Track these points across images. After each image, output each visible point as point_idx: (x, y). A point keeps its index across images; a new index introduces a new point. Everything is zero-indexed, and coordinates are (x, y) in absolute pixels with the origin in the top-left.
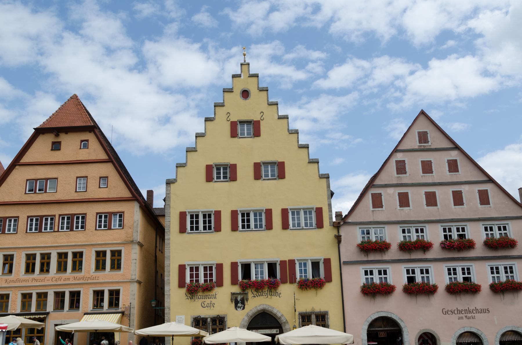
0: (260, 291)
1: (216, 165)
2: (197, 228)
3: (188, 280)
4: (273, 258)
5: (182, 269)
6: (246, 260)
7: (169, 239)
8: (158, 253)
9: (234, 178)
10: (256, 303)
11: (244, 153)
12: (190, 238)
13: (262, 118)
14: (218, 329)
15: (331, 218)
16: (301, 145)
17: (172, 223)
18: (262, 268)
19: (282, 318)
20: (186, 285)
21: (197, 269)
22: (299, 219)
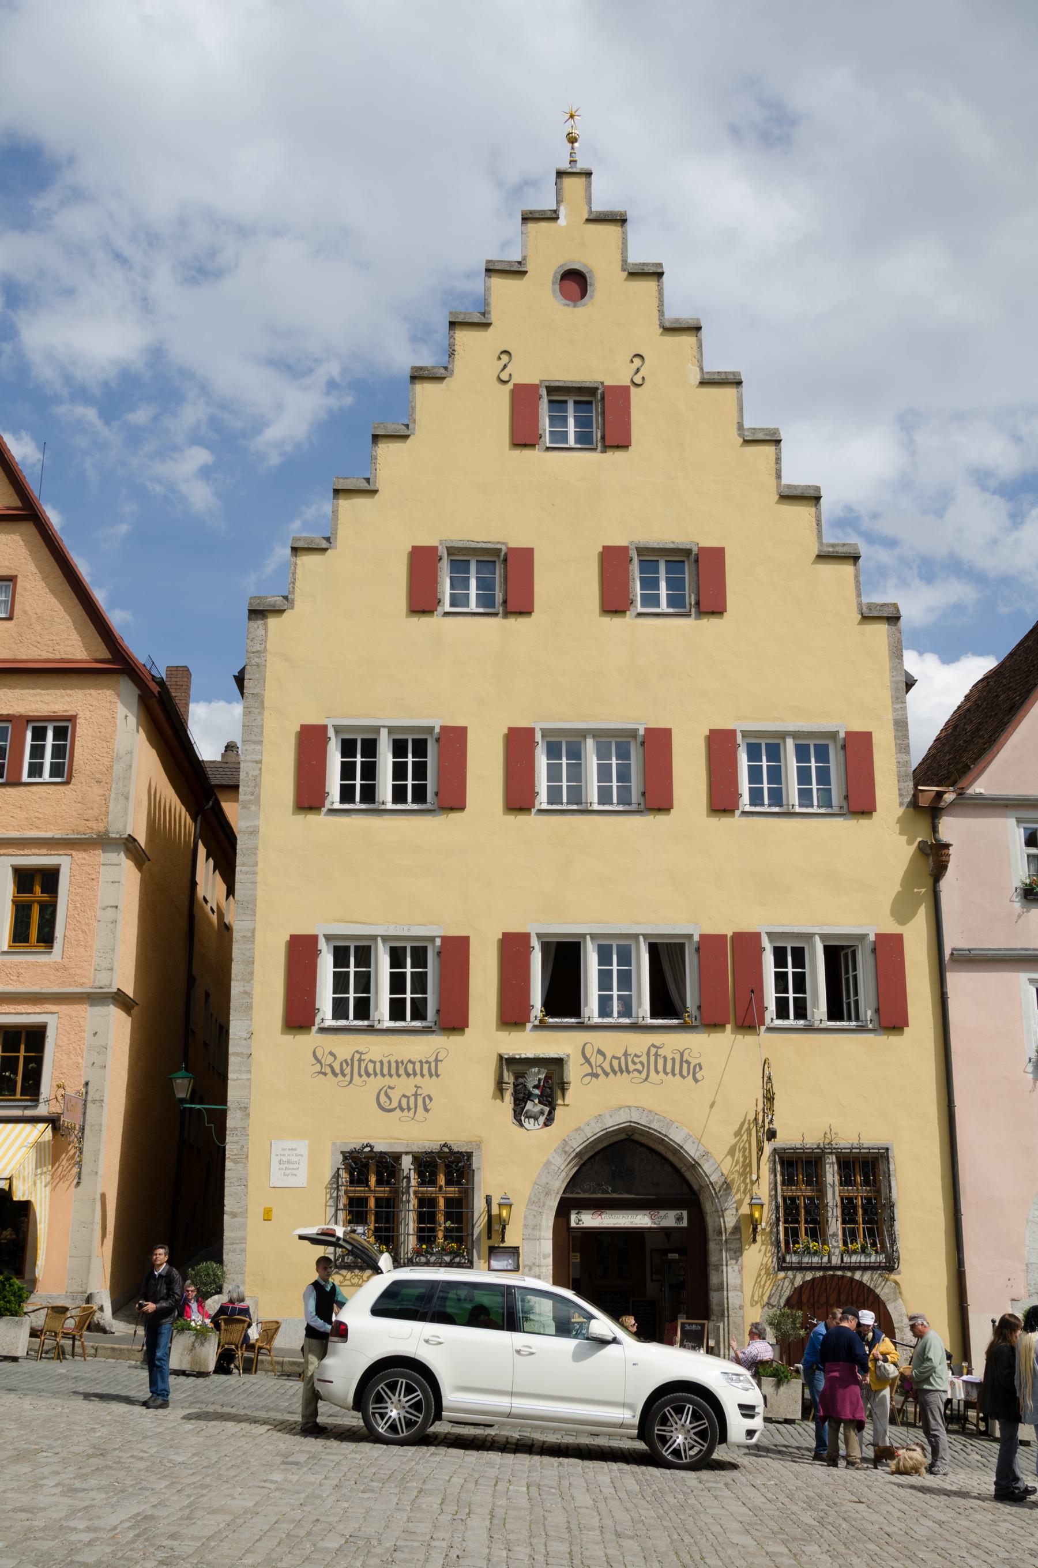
1: (451, 551)
2: (369, 794)
4: (671, 923)
6: (563, 927)
12: (338, 830)
13: (638, 380)
16: (789, 486)
19: (707, 1167)
21: (364, 955)
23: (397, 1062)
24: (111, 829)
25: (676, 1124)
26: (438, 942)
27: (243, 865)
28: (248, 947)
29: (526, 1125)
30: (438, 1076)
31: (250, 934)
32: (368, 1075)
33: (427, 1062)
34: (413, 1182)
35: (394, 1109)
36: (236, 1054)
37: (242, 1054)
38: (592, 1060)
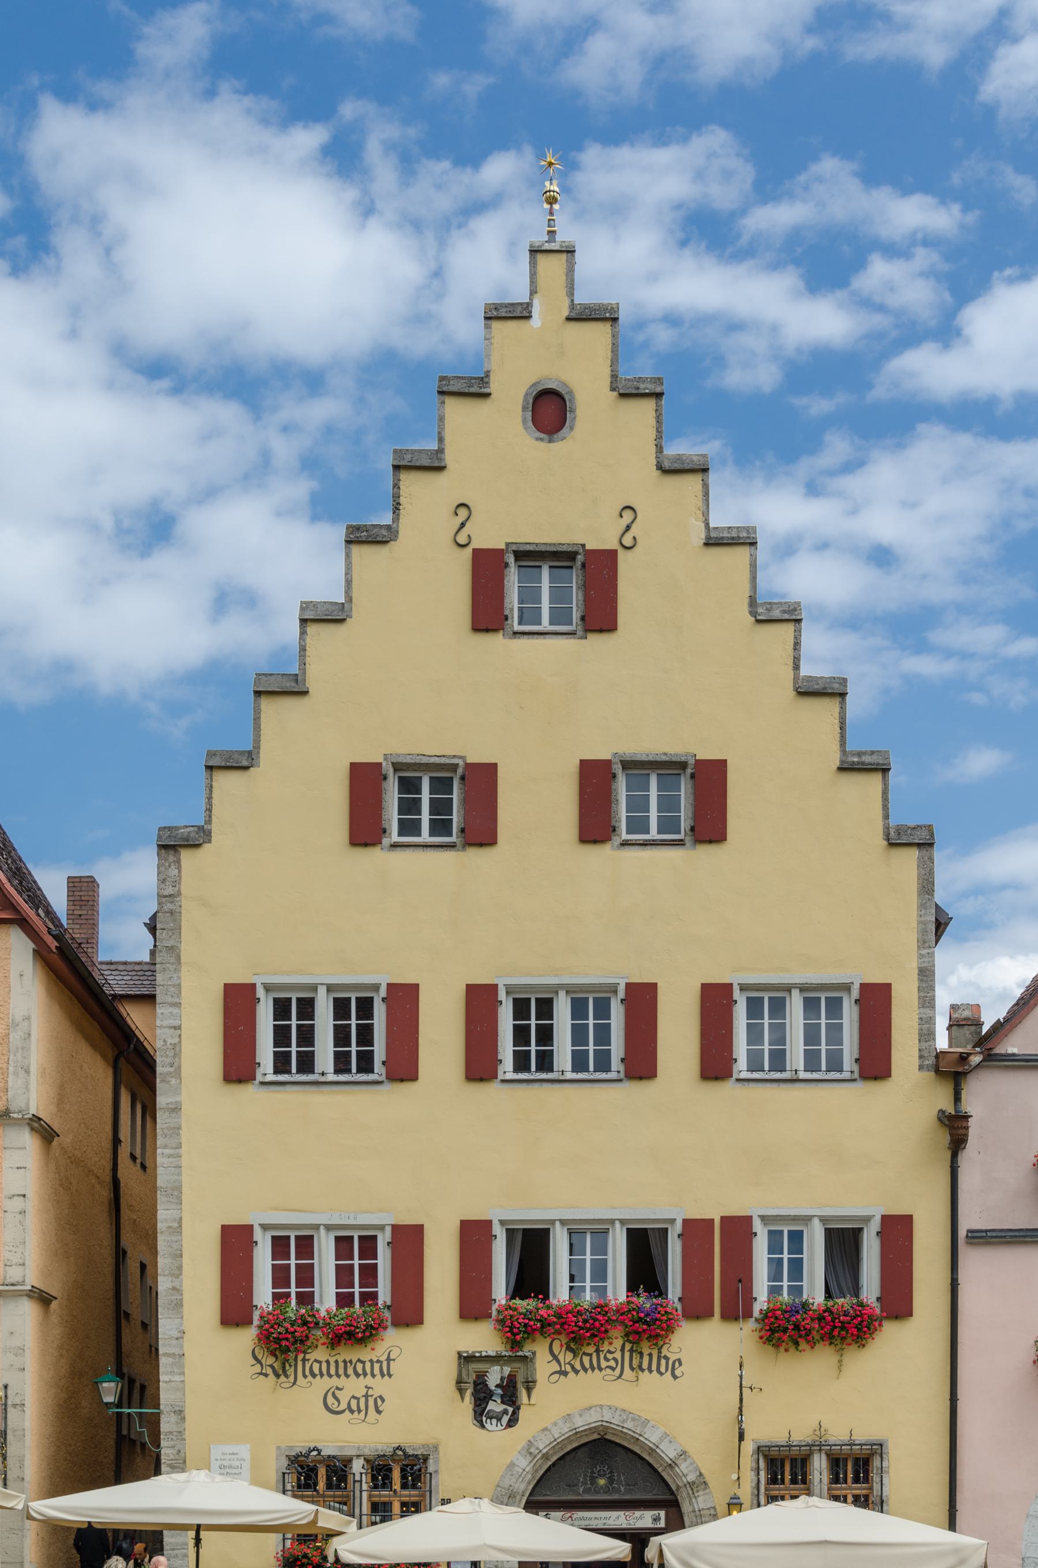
0: (591, 1349)
2: (307, 1063)
3: (263, 1294)
5: (236, 1242)
7: (176, 1109)
8: (127, 1171)
9: (481, 834)
10: (568, 1398)
11: (536, 709)
14: (396, 1508)
15: (927, 1034)
17: (187, 1035)
18: (601, 1248)
20: (256, 1315)
21: (306, 1245)
22: (779, 1035)
23: (345, 1361)
24: (12, 1108)
25: (652, 1423)
26: (388, 1229)
27: (165, 1147)
28: (175, 1239)
29: (488, 1426)
30: (390, 1376)
31: (176, 1225)
32: (314, 1376)
33: (378, 1361)
34: (365, 1487)
35: (343, 1412)
36: (166, 1354)
37: (174, 1354)
38: (561, 1357)
